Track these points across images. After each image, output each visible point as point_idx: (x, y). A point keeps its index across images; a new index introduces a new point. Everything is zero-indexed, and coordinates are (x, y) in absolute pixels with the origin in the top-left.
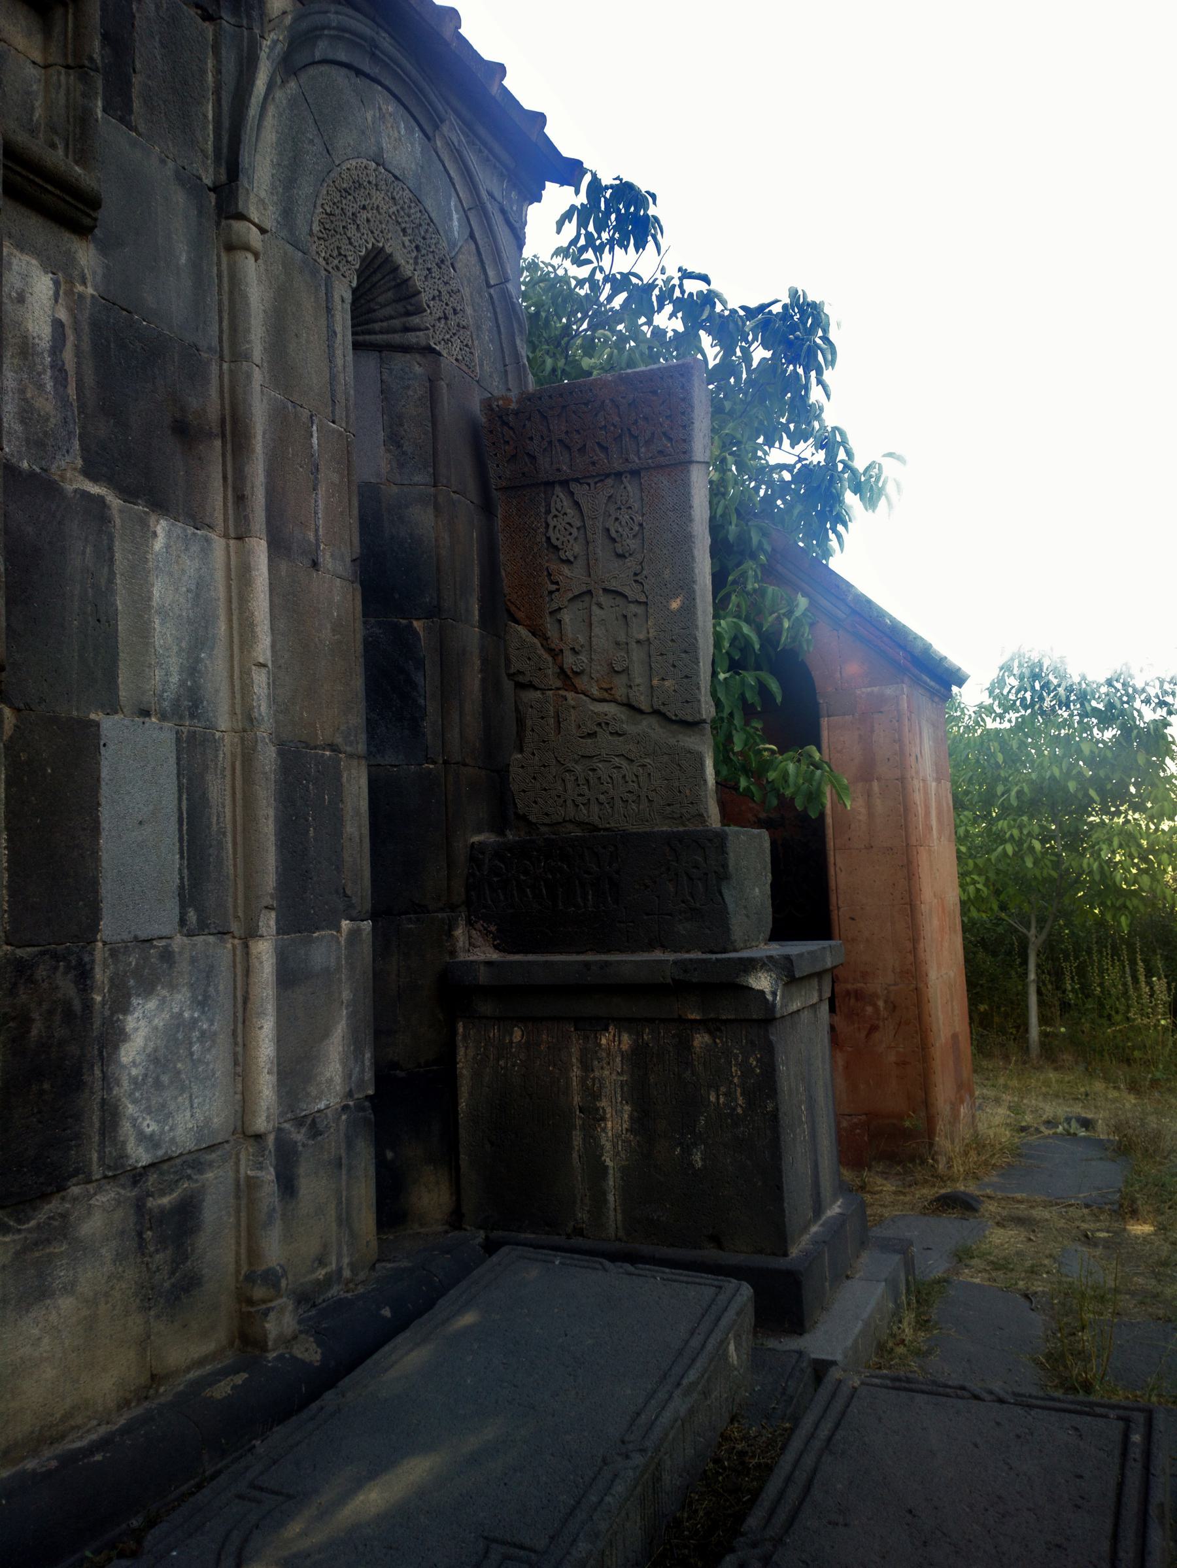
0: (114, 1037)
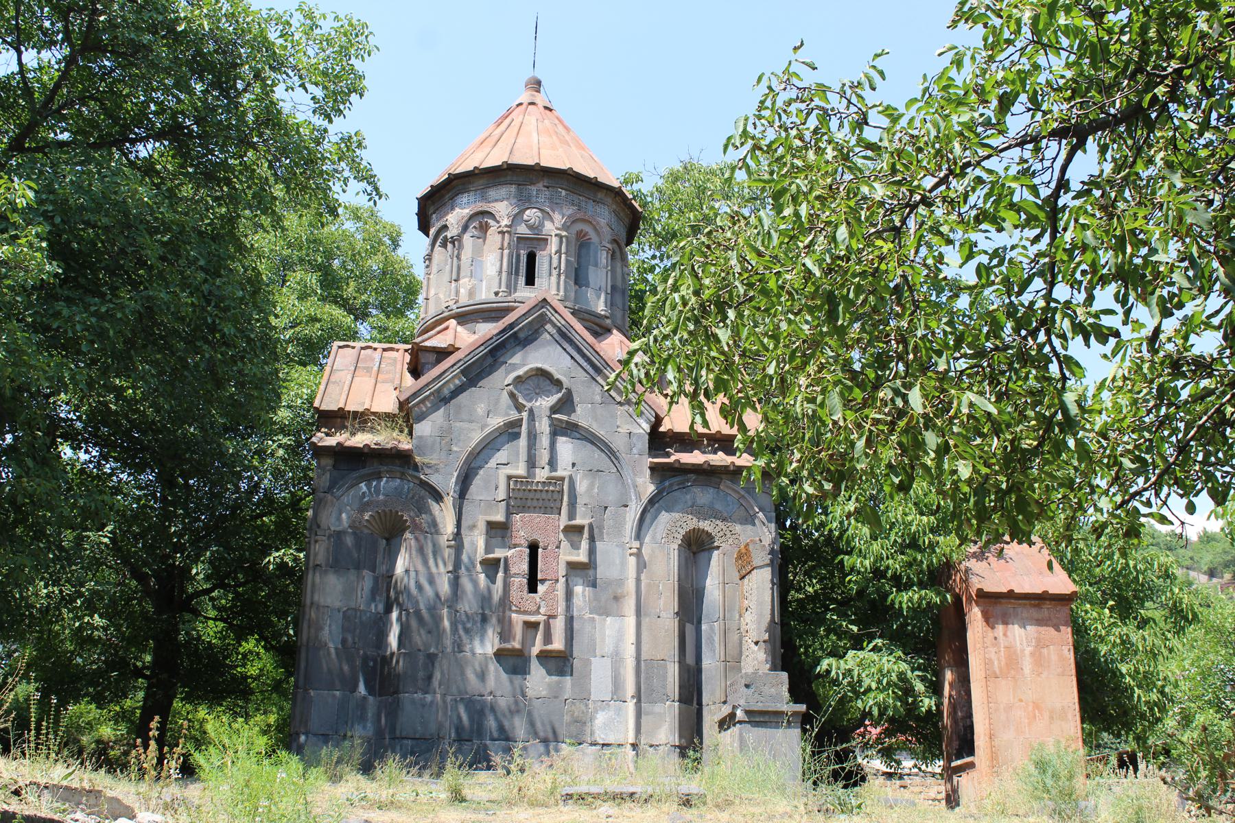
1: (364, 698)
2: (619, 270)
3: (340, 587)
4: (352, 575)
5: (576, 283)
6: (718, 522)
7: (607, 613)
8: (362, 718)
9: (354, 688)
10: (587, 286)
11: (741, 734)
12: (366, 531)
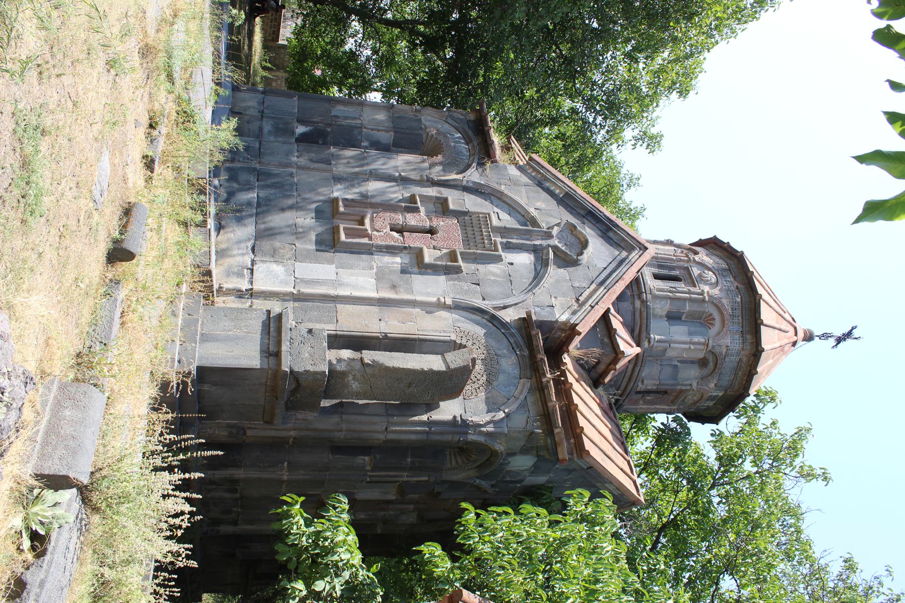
1: (293, 133)
6: (485, 378)
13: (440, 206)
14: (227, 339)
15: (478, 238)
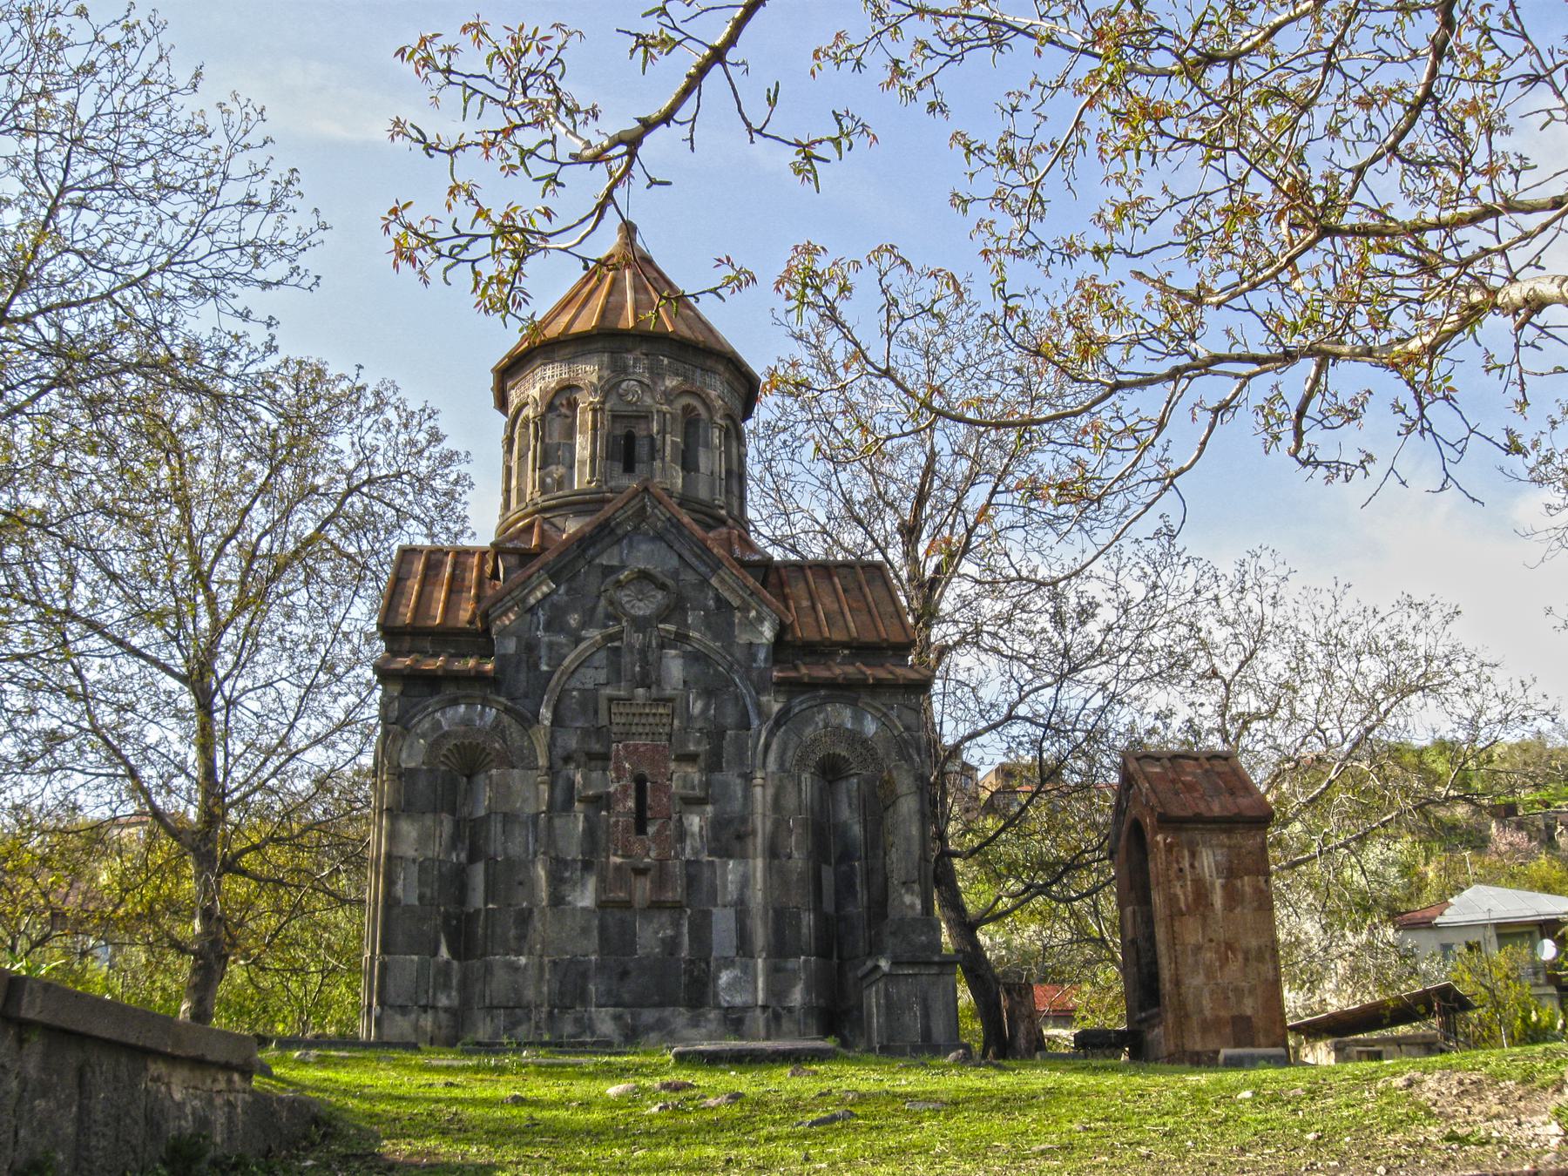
0: (719, 978)
1: (448, 962)
2: (734, 450)
3: (414, 834)
4: (429, 820)
5: (683, 468)
7: (726, 854)
8: (446, 986)
9: (436, 952)
10: (697, 470)
11: (887, 990)
12: (443, 768)
13: (593, 764)
14: (926, 1015)
15: (651, 720)
